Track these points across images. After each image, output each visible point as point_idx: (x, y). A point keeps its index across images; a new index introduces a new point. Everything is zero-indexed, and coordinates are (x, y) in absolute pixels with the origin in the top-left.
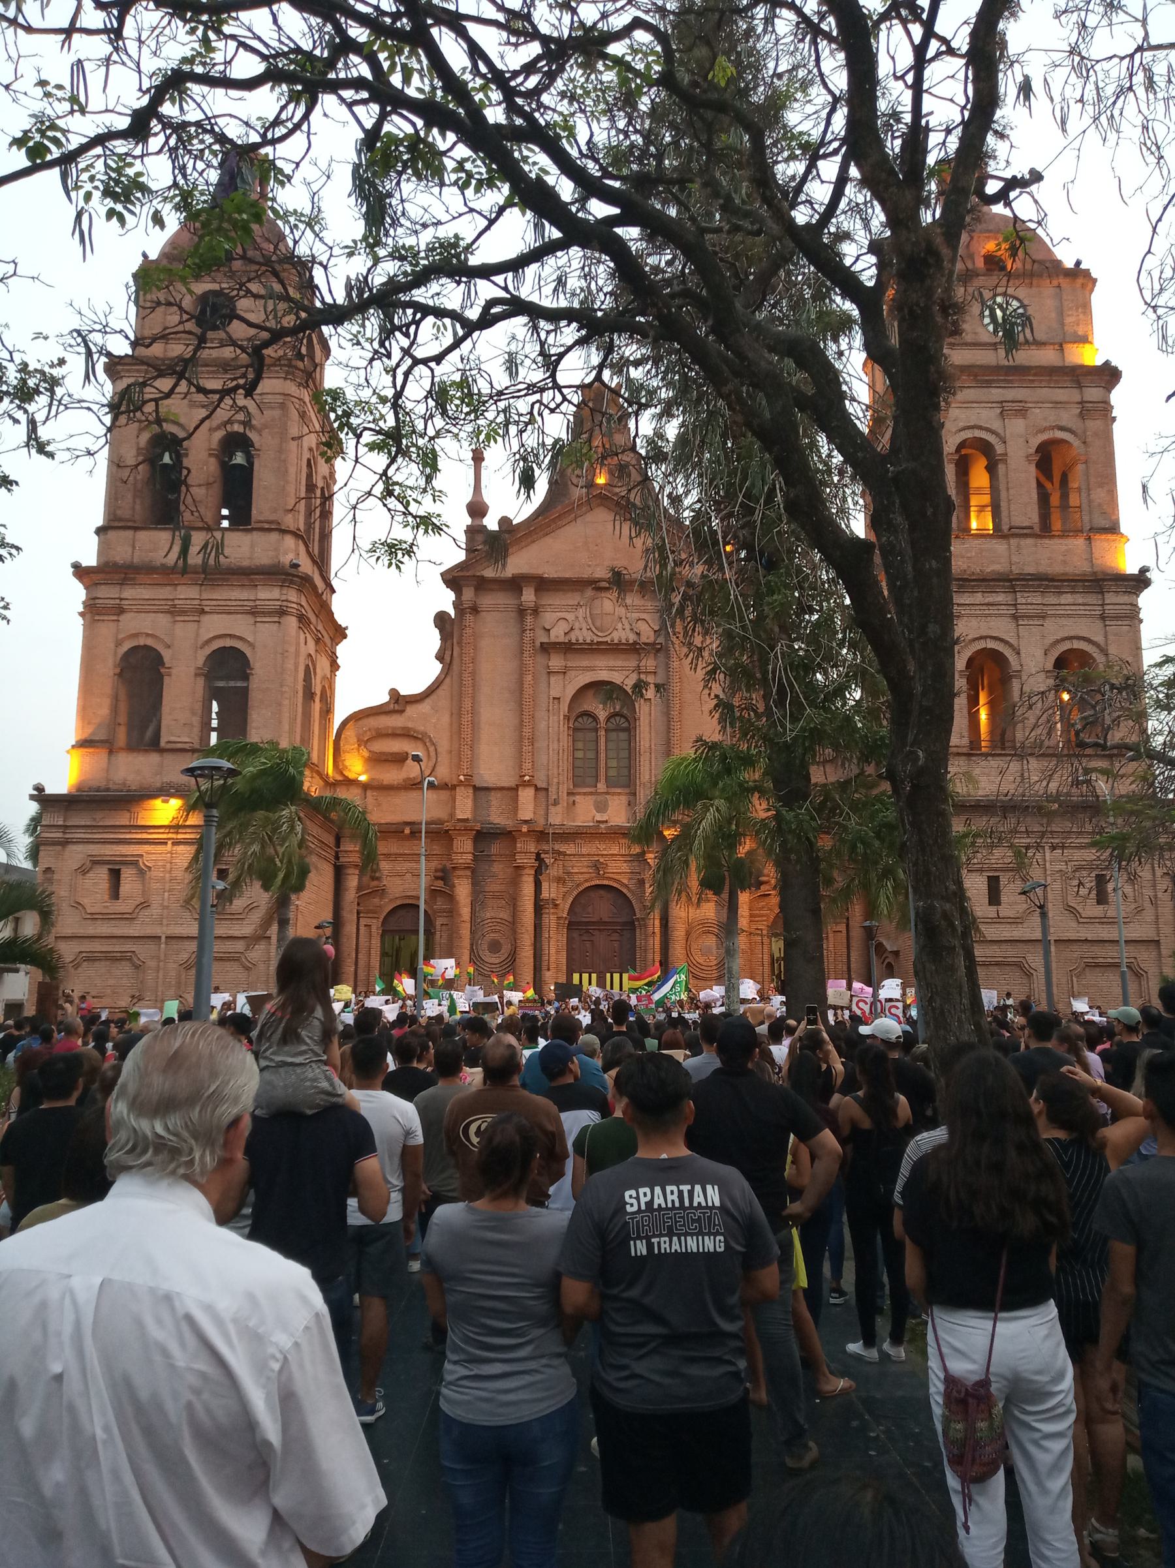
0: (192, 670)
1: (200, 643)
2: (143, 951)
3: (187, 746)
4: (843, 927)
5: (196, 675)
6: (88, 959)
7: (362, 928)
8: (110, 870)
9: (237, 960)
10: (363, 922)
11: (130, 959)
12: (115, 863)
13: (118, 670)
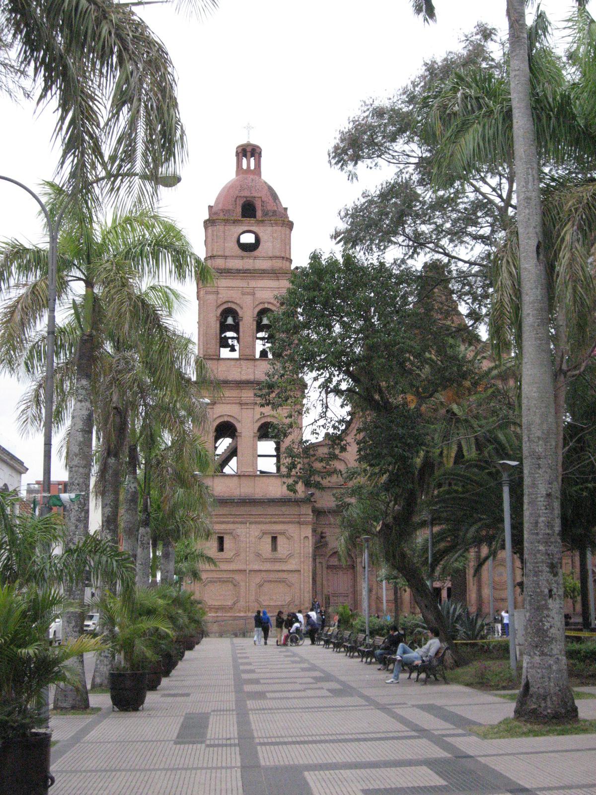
0: (252, 434)
1: (255, 420)
2: (238, 577)
3: (251, 474)
4: (570, 561)
5: (254, 437)
6: (211, 582)
7: (318, 565)
8: (219, 537)
9: (284, 582)
10: (318, 561)
11: (232, 582)
12: (221, 533)
13: (215, 434)
